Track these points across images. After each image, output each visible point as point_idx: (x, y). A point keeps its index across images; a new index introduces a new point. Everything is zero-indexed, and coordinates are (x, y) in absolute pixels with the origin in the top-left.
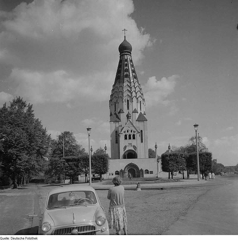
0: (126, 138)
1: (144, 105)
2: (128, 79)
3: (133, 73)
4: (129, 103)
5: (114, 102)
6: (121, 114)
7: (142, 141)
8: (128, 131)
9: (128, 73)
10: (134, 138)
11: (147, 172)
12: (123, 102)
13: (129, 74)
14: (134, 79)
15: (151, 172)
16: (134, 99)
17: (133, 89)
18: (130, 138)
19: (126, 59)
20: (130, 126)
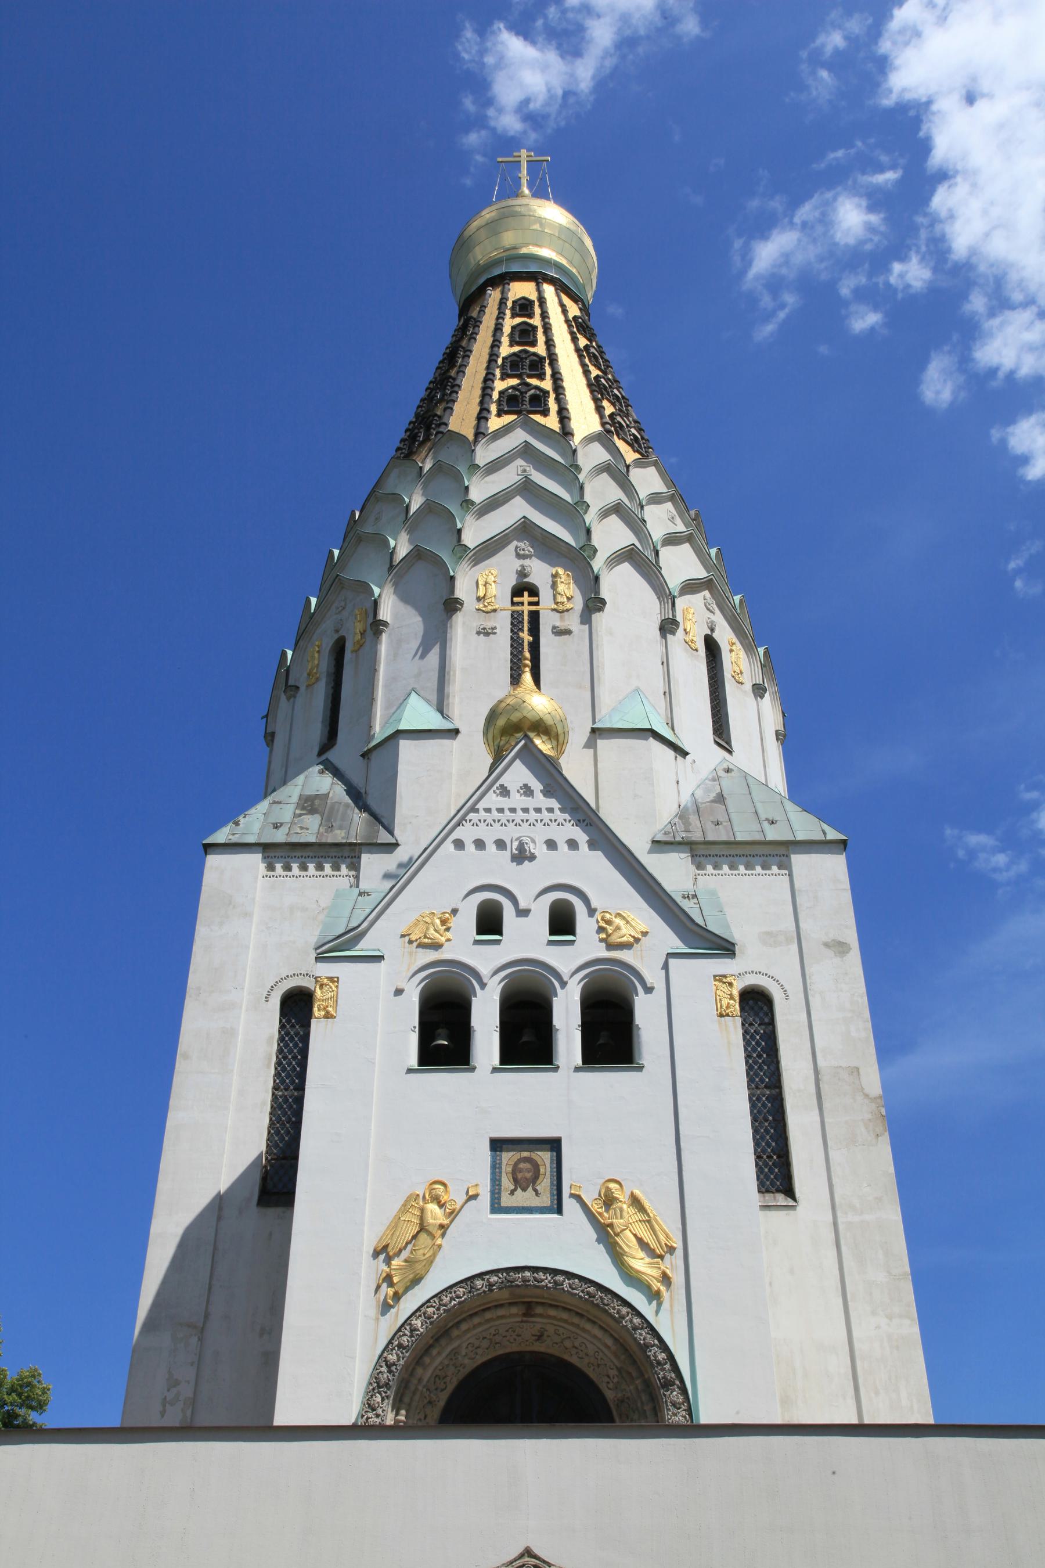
5: (328, 643)
6: (404, 744)
7: (776, 1174)
8: (490, 923)
10: (611, 1036)
12: (452, 605)
20: (536, 838)
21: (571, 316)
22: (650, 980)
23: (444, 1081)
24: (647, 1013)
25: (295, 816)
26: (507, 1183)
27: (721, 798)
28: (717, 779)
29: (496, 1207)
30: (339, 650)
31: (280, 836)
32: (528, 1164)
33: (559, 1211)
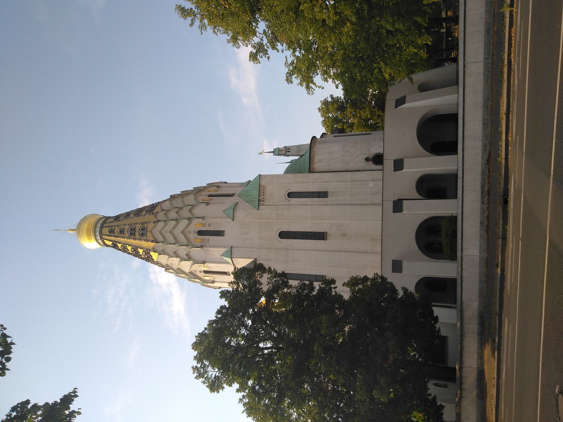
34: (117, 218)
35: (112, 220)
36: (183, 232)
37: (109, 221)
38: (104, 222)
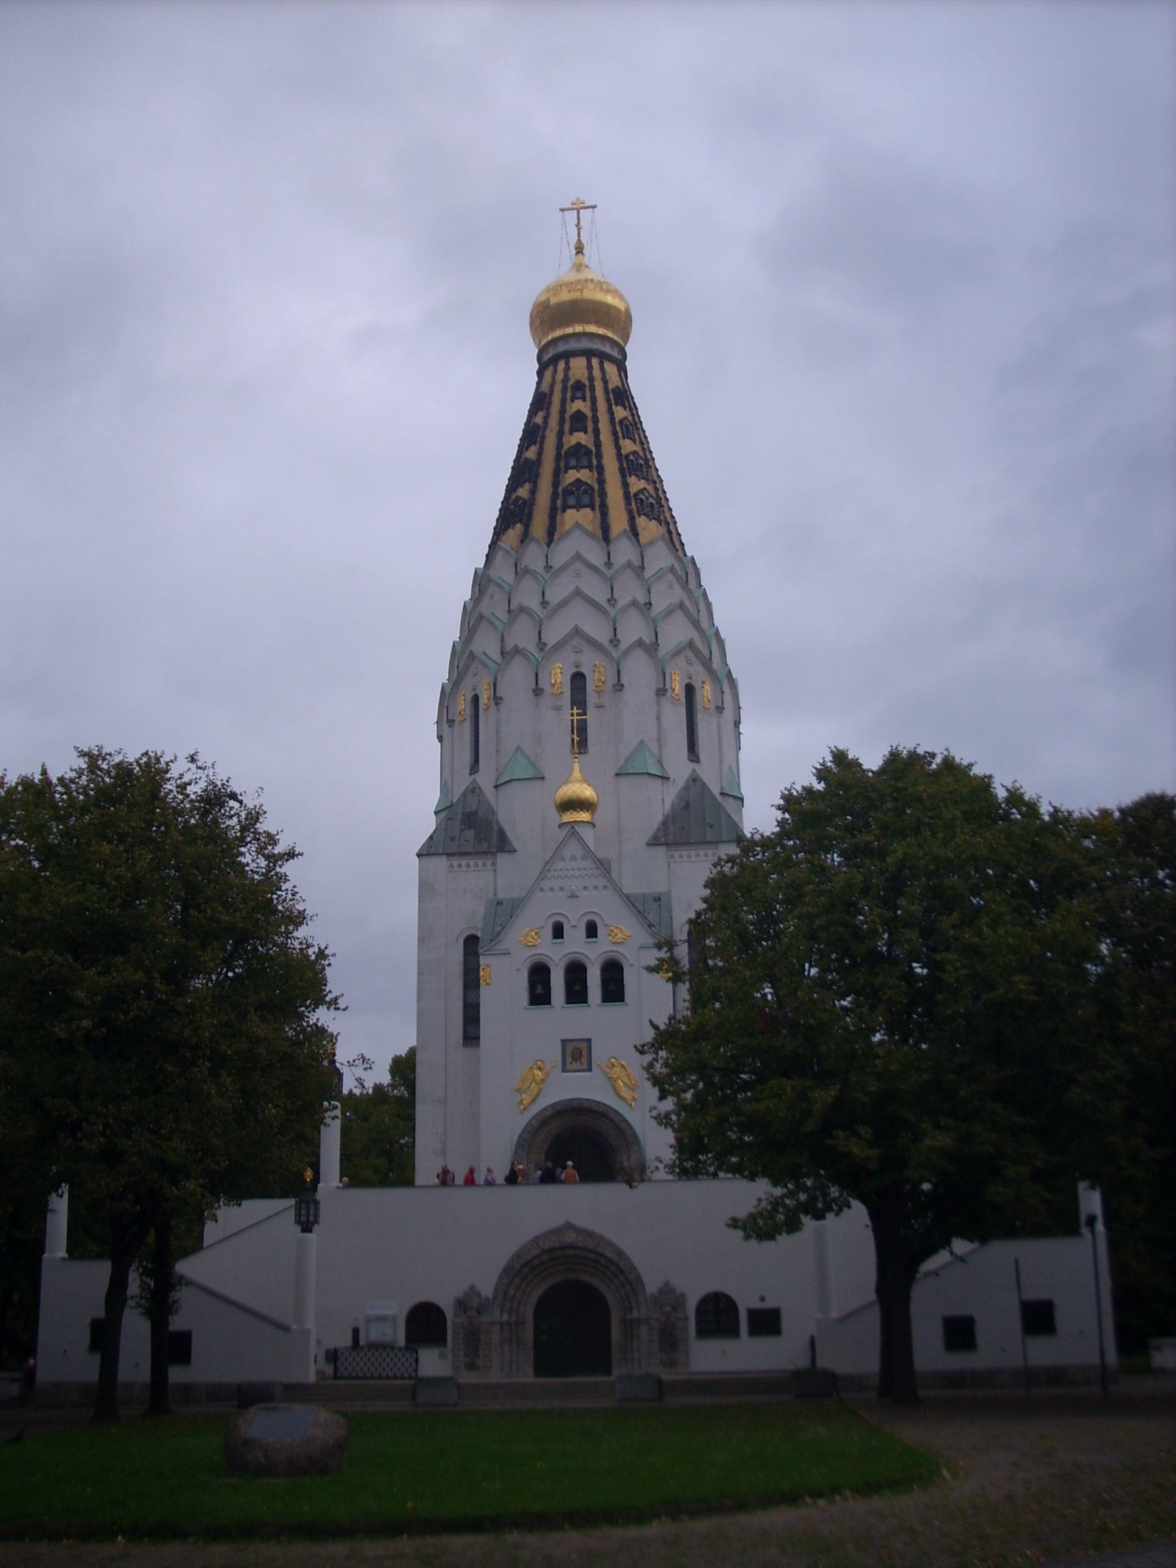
0: (539, 995)
1: (728, 714)
2: (586, 517)
3: (632, 480)
4: (591, 698)
5: (470, 697)
8: (558, 932)
9: (584, 475)
10: (614, 990)
11: (718, 1316)
13: (601, 481)
14: (641, 521)
15: (766, 1322)
16: (639, 672)
17: (629, 590)
18: (576, 993)
19: (578, 386)
21: (611, 386)
22: (631, 961)
23: (541, 1011)
24: (630, 978)
25: (462, 830)
26: (569, 1059)
27: (687, 807)
28: (686, 788)
29: (564, 1070)
30: (476, 699)
31: (453, 848)
32: (577, 1054)
33: (590, 1070)
34: (622, 396)
35: (614, 382)
36: (577, 632)
37: (611, 369)
38: (603, 357)
